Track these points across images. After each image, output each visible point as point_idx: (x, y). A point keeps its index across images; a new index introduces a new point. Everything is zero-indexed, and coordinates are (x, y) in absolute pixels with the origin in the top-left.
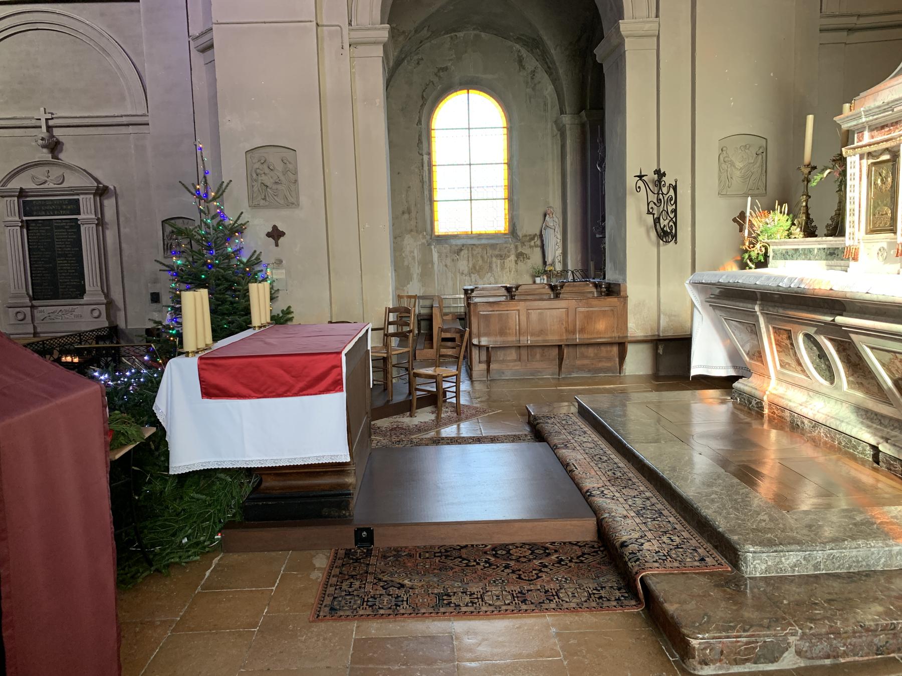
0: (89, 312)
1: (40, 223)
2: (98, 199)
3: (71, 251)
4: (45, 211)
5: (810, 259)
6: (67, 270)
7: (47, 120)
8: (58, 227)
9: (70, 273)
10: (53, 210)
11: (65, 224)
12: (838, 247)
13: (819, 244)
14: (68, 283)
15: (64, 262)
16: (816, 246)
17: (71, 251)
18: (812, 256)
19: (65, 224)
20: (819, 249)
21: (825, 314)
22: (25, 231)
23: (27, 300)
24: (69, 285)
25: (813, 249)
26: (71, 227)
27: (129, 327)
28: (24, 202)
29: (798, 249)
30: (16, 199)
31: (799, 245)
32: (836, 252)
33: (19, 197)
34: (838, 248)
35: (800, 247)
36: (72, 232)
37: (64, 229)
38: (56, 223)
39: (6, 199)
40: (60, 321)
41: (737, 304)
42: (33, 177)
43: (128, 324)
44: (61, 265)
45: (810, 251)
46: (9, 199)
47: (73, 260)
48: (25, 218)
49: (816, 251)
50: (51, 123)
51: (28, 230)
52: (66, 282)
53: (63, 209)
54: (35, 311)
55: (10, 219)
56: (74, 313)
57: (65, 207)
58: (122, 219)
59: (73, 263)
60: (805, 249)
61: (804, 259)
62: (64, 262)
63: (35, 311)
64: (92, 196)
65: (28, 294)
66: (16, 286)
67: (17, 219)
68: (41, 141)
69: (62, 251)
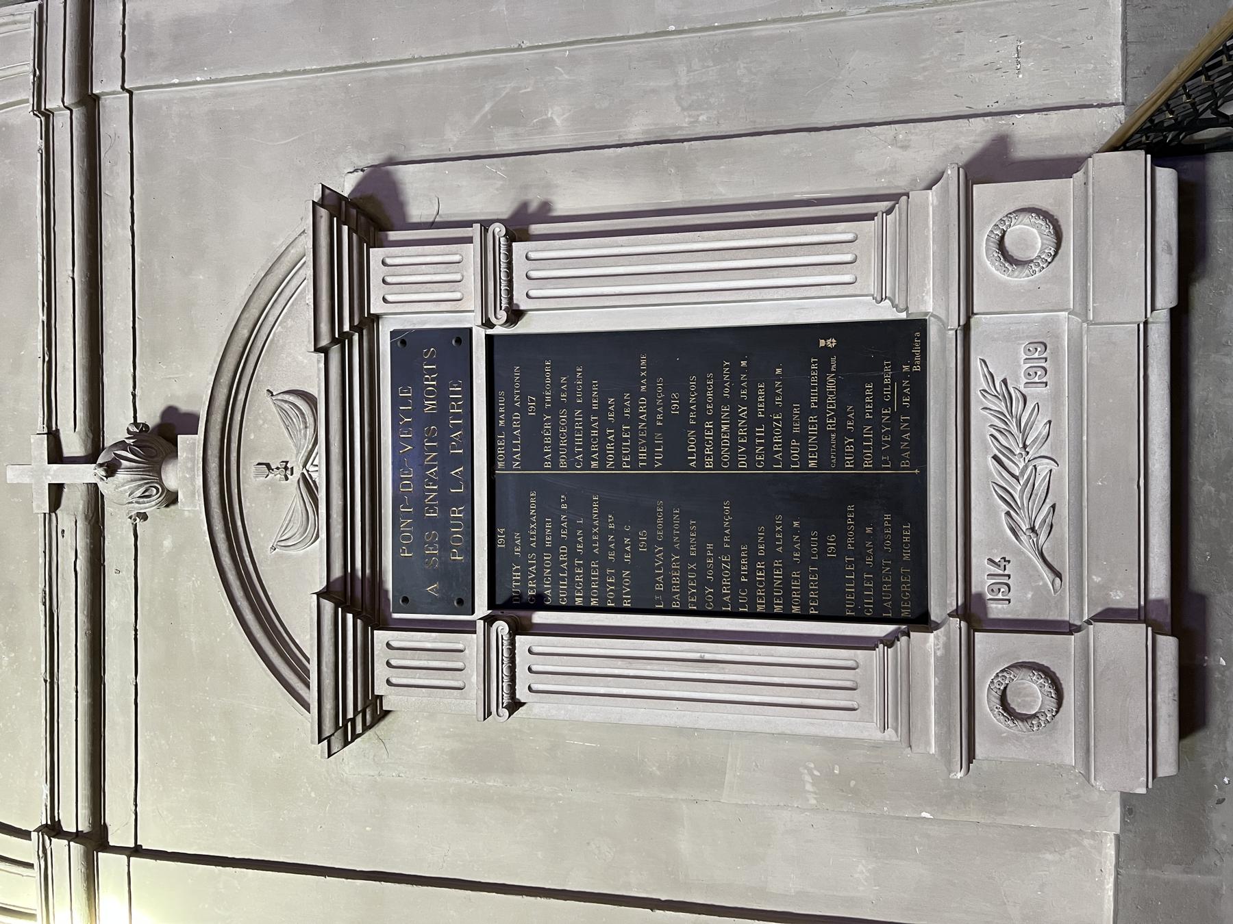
0: (1018, 279)
1: (510, 540)
2: (393, 235)
3: (651, 395)
4: (446, 502)
6: (753, 421)
7: (56, 455)
8: (533, 456)
9: (770, 407)
10: (448, 462)
11: (517, 416)
14: (831, 424)
15: (709, 435)
17: (651, 395)
19: (517, 416)
22: (540, 617)
23: (929, 644)
24: (841, 414)
26: (532, 385)
27: (1117, 93)
28: (406, 602)
30: (381, 636)
33: (375, 618)
36: (556, 385)
37: (538, 423)
38: (508, 467)
39: (380, 688)
40: (1064, 470)
42: (283, 543)
43: (1102, 98)
44: (726, 456)
46: (381, 672)
47: (702, 389)
48: (482, 608)
50: (73, 444)
51: (540, 603)
52: (823, 433)
53: (441, 416)
54: (997, 610)
55: (474, 678)
56: (1020, 382)
57: (430, 405)
58: (503, 141)
59: (719, 387)
62: (709, 435)
63: (997, 610)
64: (376, 254)
65: (889, 642)
66: (840, 699)
67: (472, 643)
68: (121, 476)
69: (651, 446)
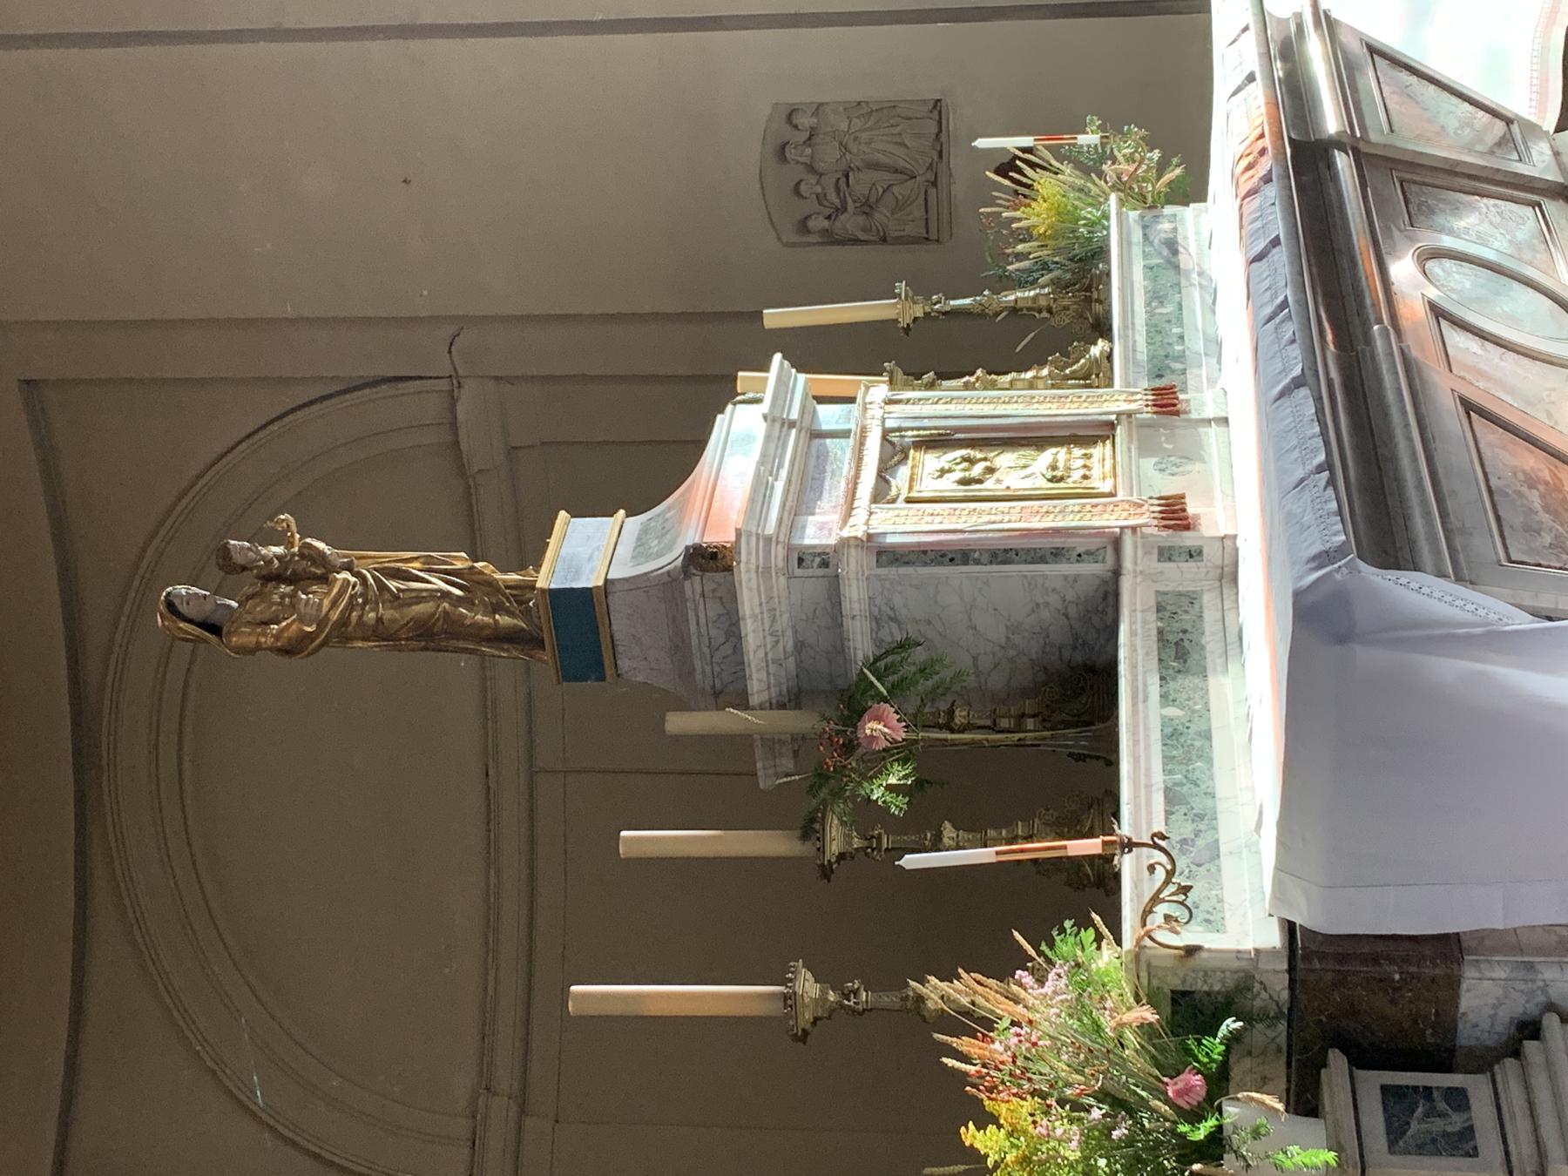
5: (1207, 736)
12: (1154, 632)
13: (1145, 700)
16: (1155, 712)
18: (1194, 728)
20: (1165, 697)
21: (1335, 177)
25: (1163, 718)
29: (1167, 790)
31: (1149, 786)
32: (1173, 638)
34: (1160, 632)
35: (1158, 779)
41: (1390, 396)
45: (1172, 735)
49: (1172, 711)
60: (1167, 759)
61: (1210, 761)
